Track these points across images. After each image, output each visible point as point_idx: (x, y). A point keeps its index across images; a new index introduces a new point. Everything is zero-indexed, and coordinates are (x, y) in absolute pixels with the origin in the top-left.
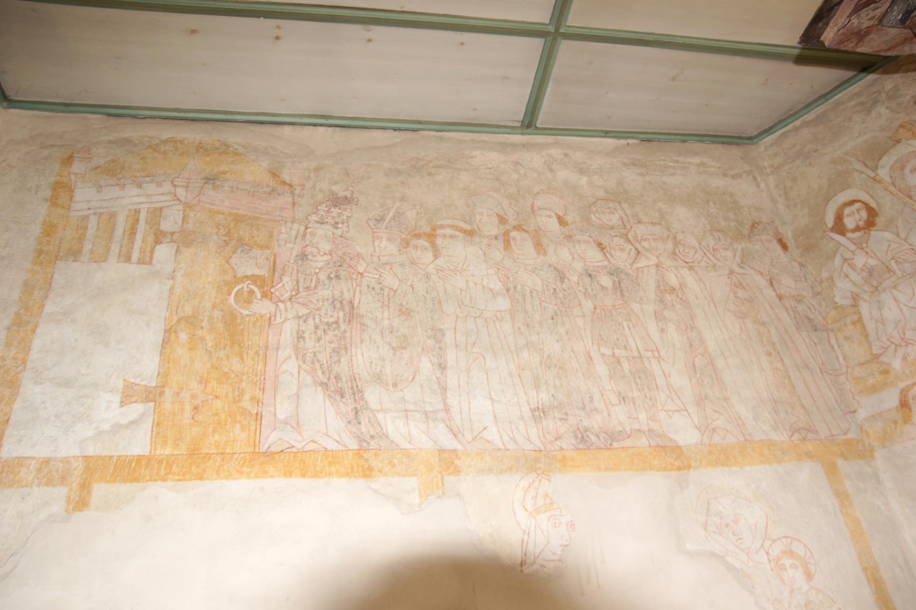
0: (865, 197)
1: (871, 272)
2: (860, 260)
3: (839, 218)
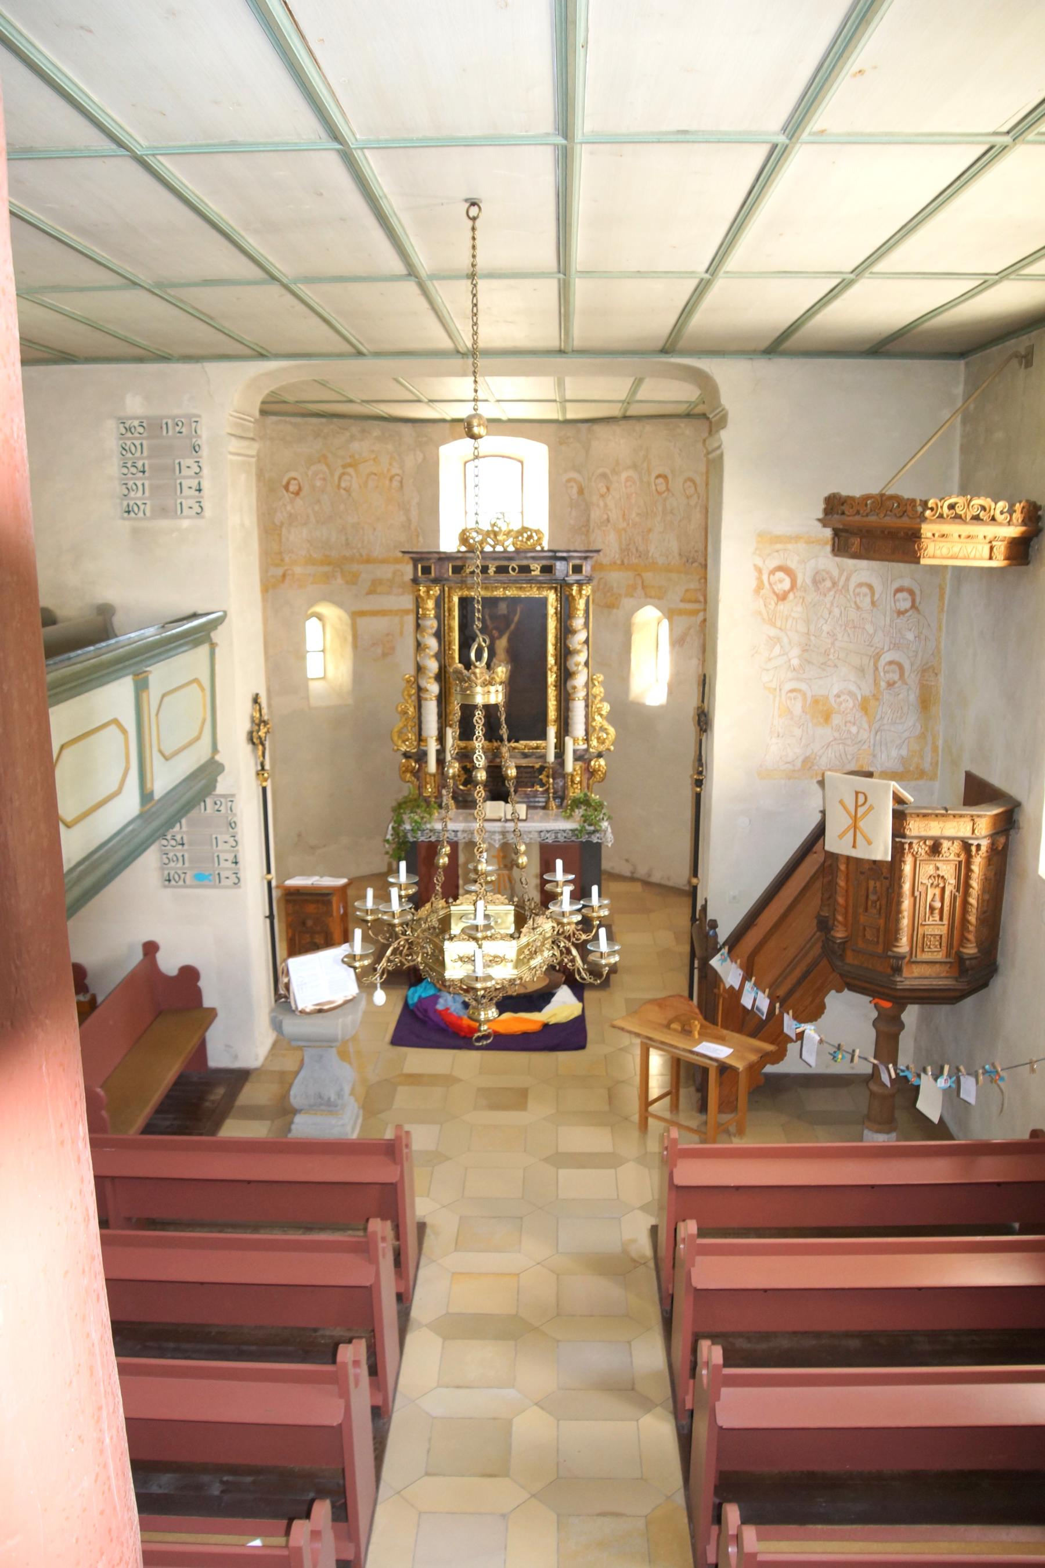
0: (299, 478)
1: (290, 515)
2: (289, 508)
3: (288, 484)
